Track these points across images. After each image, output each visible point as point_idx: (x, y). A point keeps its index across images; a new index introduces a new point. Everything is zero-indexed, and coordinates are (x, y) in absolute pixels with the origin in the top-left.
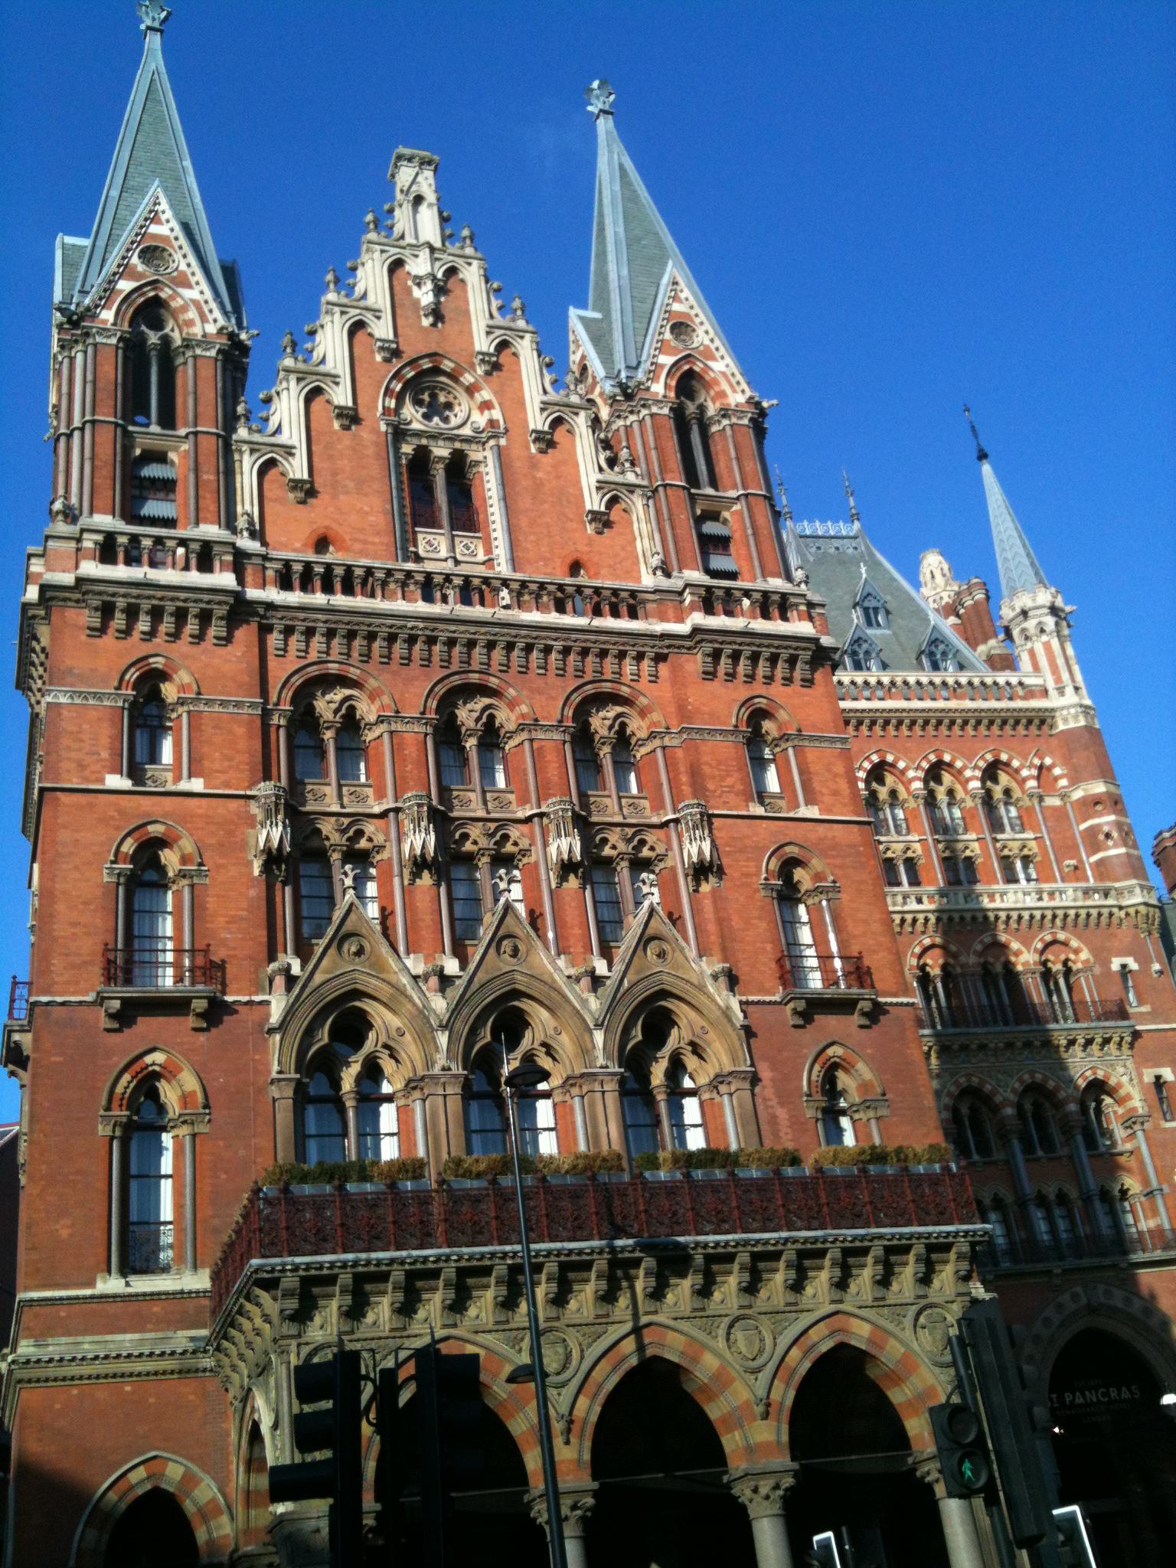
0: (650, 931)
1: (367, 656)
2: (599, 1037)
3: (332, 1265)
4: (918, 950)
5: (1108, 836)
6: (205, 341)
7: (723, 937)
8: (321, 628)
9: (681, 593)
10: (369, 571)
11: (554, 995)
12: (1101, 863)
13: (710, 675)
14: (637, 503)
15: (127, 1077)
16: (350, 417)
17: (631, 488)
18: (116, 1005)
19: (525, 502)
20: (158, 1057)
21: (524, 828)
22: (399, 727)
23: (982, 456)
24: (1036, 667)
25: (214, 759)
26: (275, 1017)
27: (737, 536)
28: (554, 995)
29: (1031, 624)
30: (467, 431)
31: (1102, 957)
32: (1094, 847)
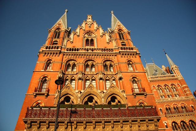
0: (112, 86)
1: (76, 57)
2: (103, 99)
3: (36, 120)
4: (165, 105)
5: (187, 91)
6: (63, 31)
7: (123, 87)
8: (71, 54)
9: (118, 49)
10: (78, 49)
11: (97, 94)
12: (186, 94)
13: (122, 57)
14: (113, 41)
15: (35, 104)
16: (79, 36)
17: (113, 40)
18: (35, 94)
19: (99, 42)
20: (40, 101)
21: (96, 75)
22: (79, 64)
23: (166, 54)
24: (175, 73)
25: (55, 68)
26: (56, 96)
27: (126, 44)
28: (97, 94)
29: (174, 69)
30: (93, 37)
31: (189, 105)
32: (185, 92)
